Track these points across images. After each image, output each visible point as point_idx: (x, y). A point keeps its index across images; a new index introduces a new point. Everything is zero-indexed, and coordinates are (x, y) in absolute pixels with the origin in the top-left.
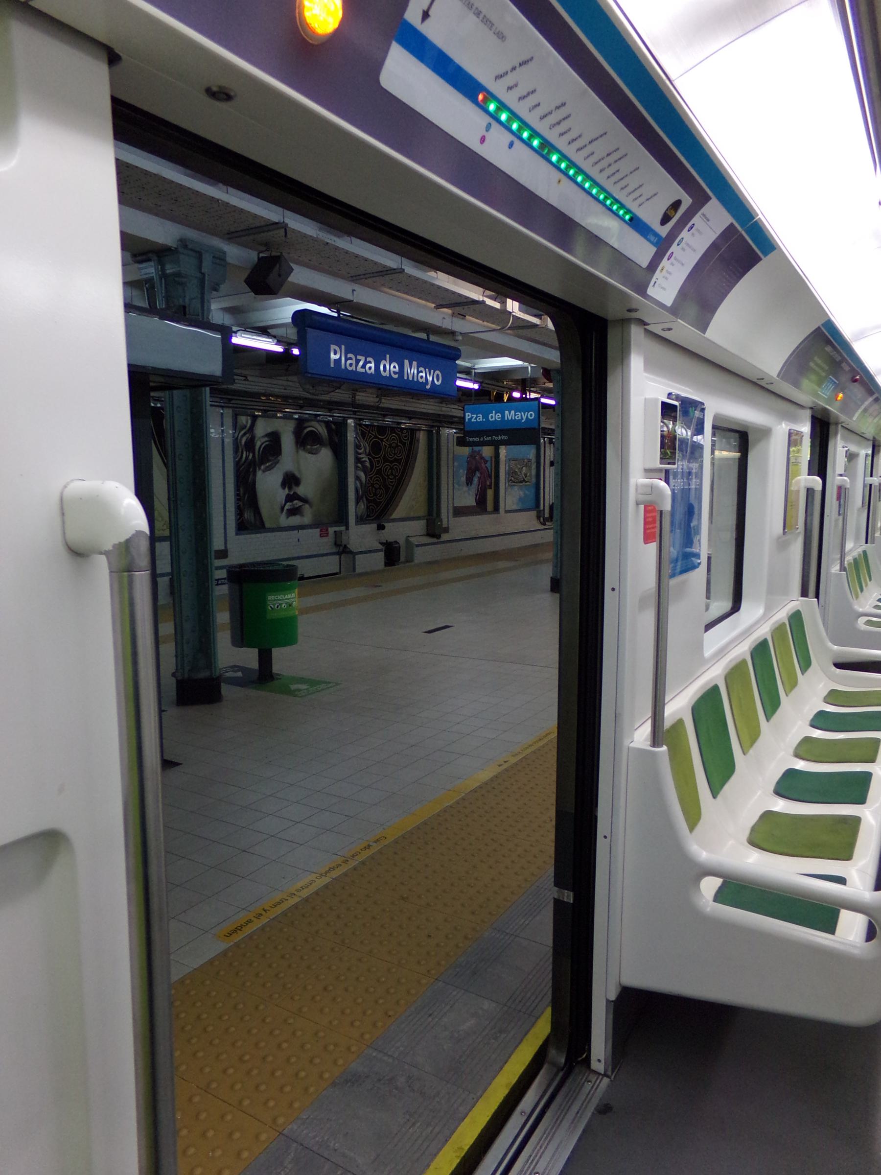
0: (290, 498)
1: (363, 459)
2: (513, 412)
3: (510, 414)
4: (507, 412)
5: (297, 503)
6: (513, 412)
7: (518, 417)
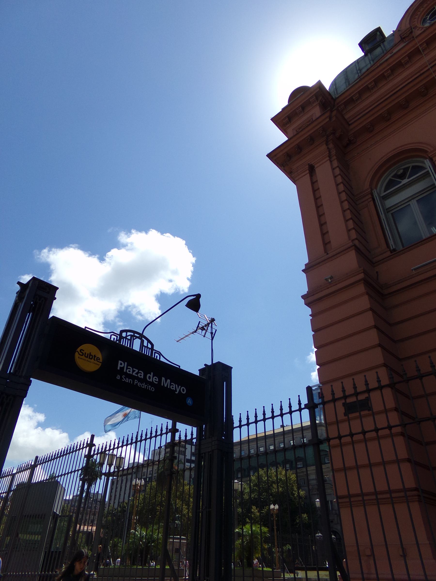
7: (173, 387)
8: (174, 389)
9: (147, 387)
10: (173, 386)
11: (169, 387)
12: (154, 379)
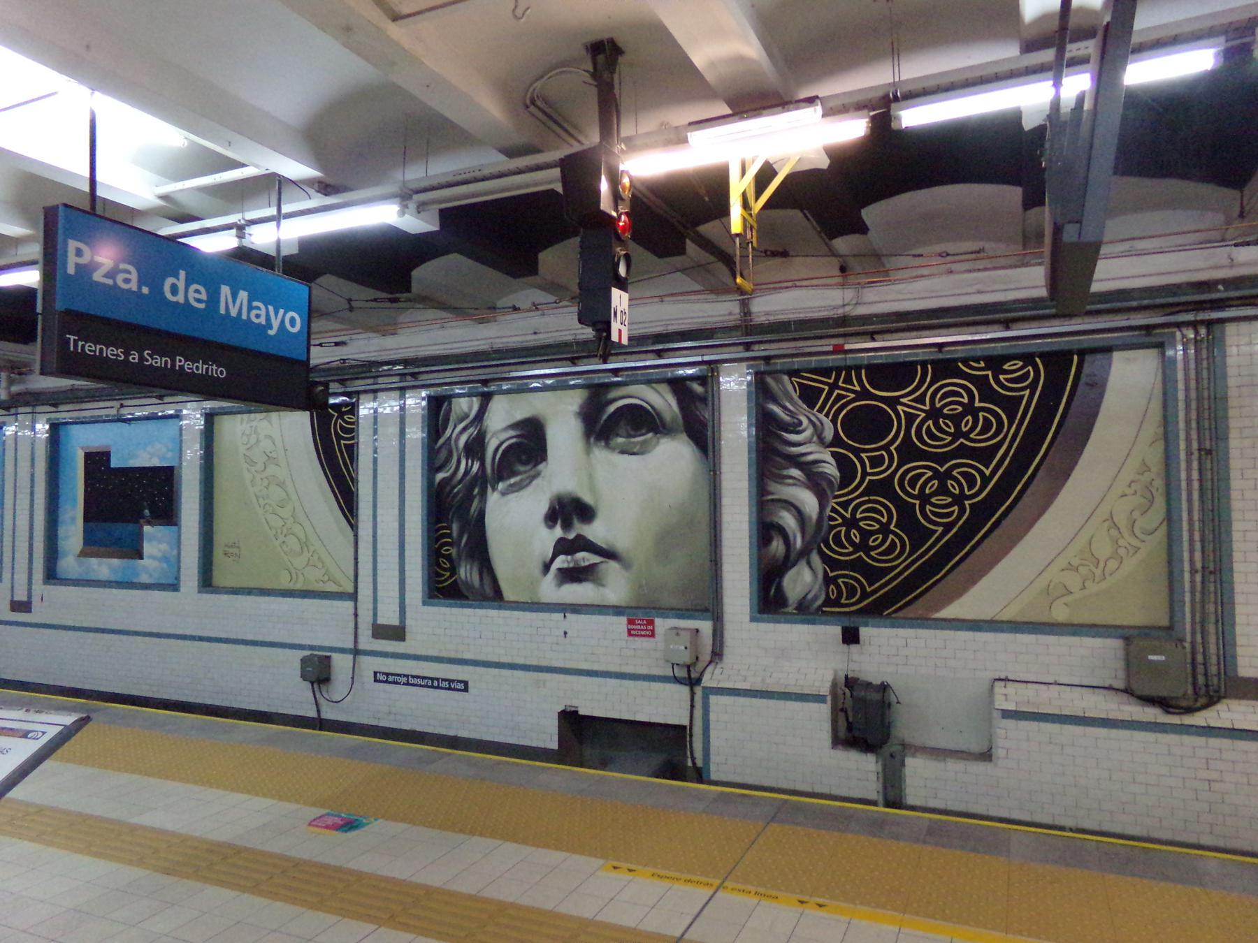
0: (563, 547)
1: (811, 458)
2: (243, 295)
3: (235, 295)
4: (225, 290)
5: (585, 558)
6: (243, 295)
7: (258, 316)
8: (264, 323)
9: (207, 369)
10: (258, 312)
11: (244, 317)
12: (191, 295)
